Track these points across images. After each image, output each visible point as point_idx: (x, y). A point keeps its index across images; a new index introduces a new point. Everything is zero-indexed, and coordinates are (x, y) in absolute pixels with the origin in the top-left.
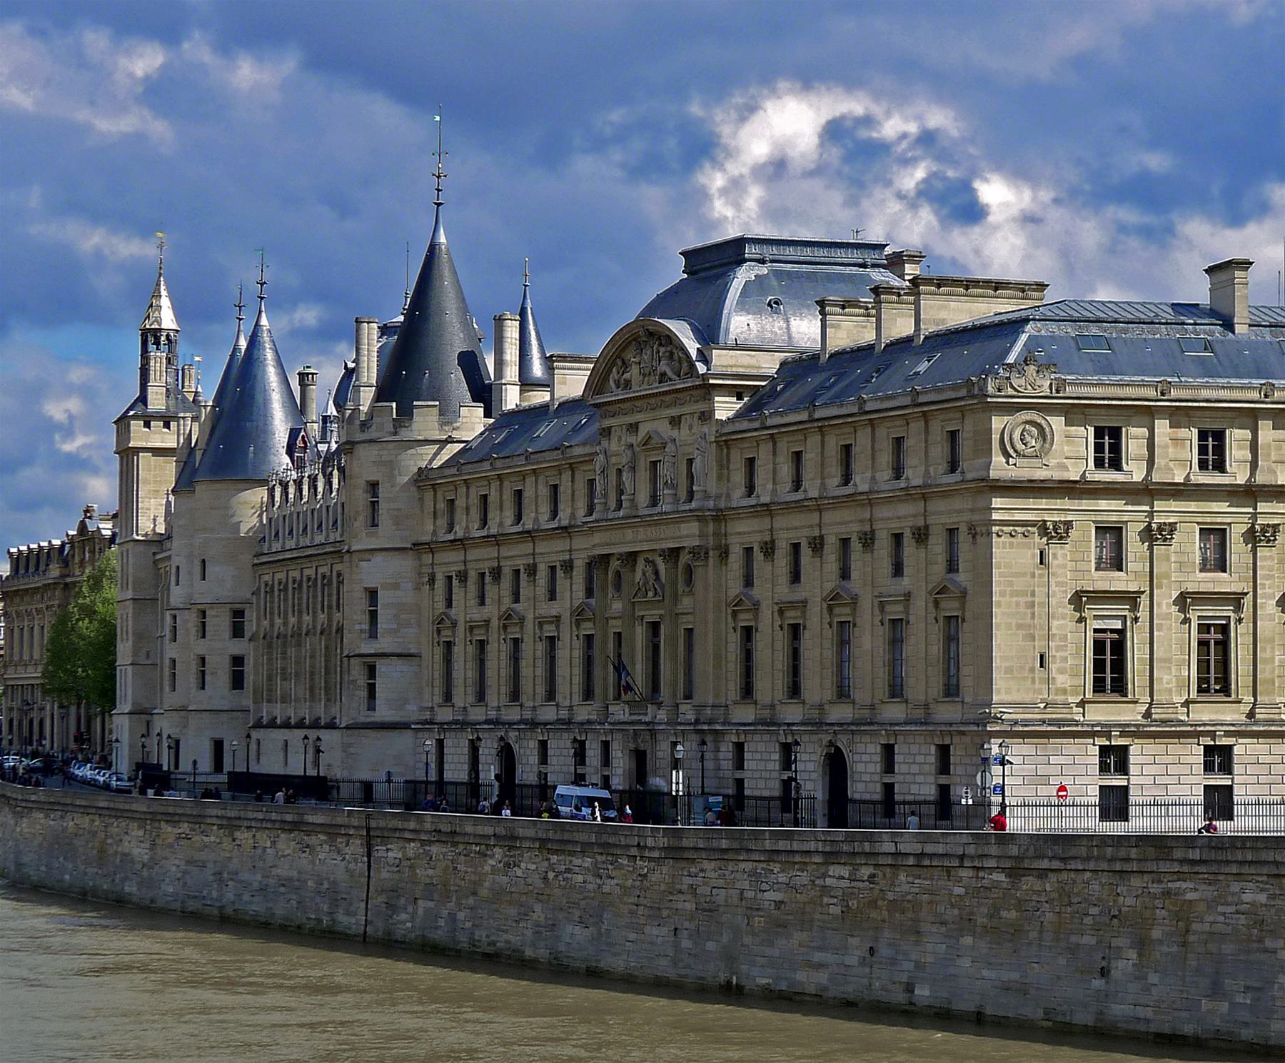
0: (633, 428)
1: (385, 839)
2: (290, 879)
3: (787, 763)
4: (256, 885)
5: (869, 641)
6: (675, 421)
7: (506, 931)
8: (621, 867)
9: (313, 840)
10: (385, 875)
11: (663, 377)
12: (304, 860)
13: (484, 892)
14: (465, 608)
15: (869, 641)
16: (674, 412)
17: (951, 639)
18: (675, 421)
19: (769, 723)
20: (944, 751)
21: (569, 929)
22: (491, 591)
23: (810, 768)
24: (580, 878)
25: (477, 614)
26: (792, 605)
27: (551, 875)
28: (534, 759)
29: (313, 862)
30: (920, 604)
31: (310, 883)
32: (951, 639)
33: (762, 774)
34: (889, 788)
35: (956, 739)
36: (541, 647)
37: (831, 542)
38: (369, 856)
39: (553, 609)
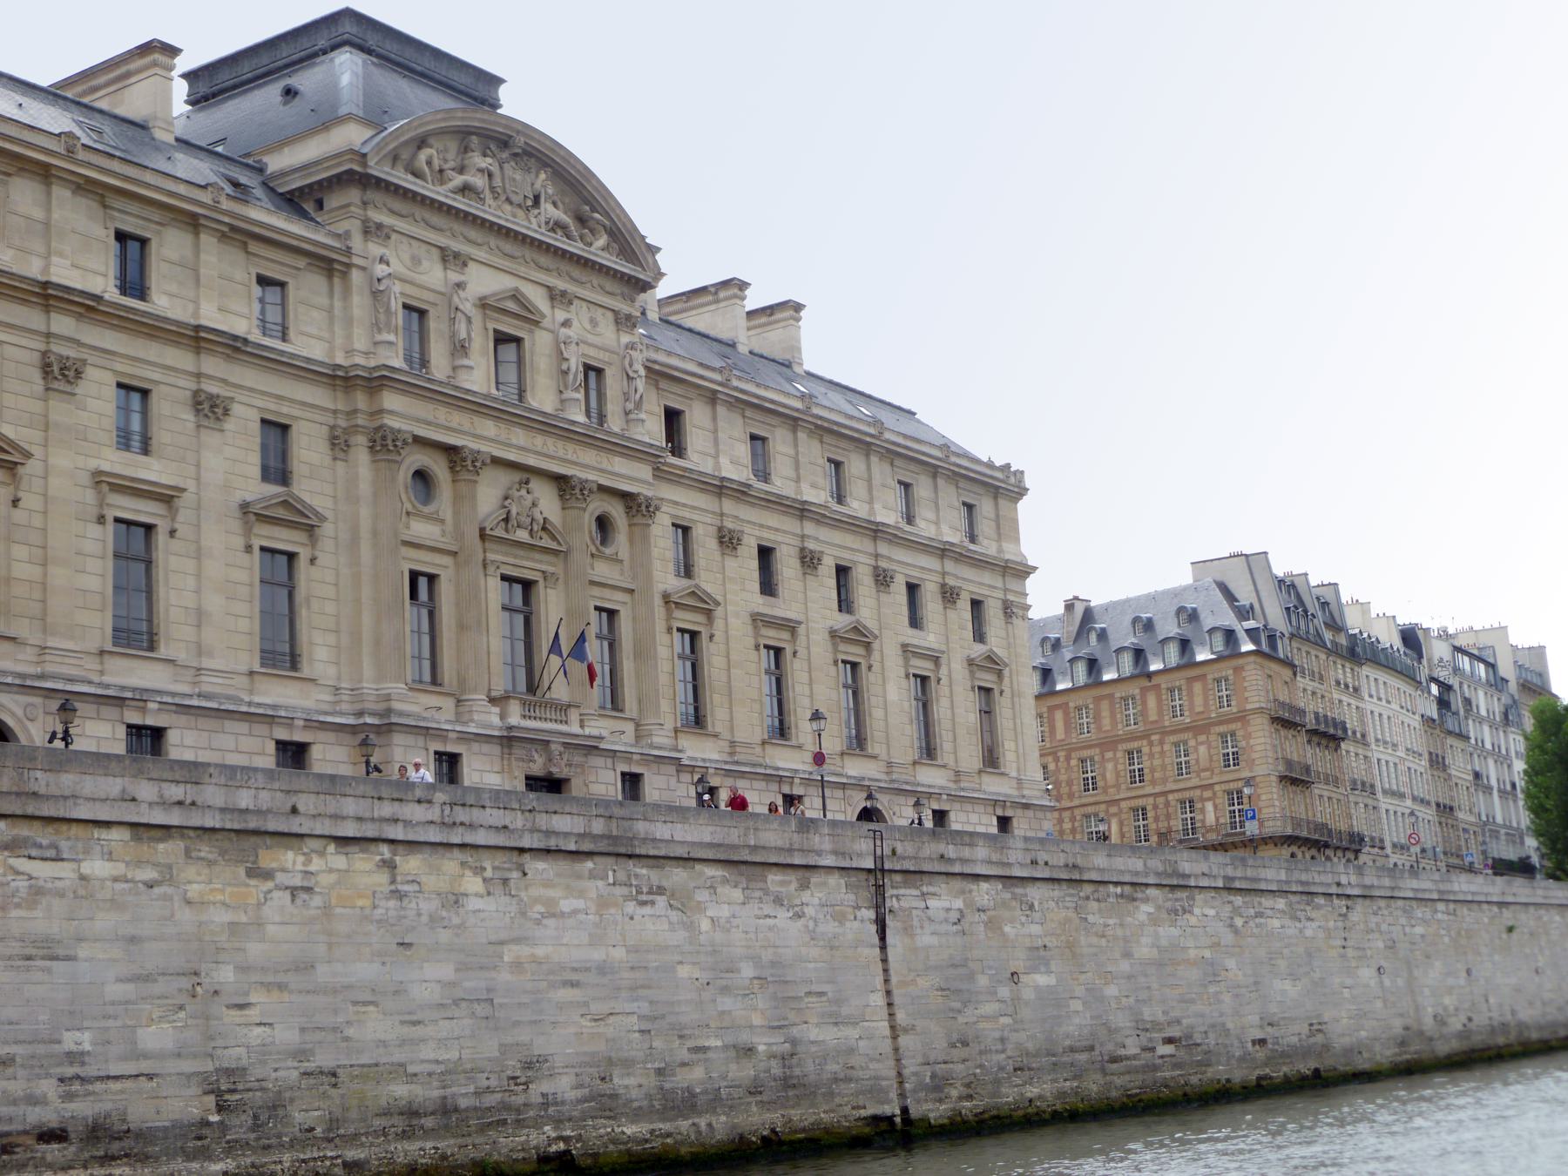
1: (913, 875)
2: (602, 969)
4: (424, 993)
7: (1192, 1001)
8: (1318, 907)
10: (925, 939)
11: (557, 226)
12: (653, 923)
13: (1144, 950)
16: (560, 284)
17: (987, 713)
21: (1278, 984)
24: (1276, 923)
27: (1239, 922)
29: (691, 927)
31: (684, 972)
32: (987, 713)
35: (1019, 812)
36: (99, 541)
38: (879, 904)
39: (152, 470)
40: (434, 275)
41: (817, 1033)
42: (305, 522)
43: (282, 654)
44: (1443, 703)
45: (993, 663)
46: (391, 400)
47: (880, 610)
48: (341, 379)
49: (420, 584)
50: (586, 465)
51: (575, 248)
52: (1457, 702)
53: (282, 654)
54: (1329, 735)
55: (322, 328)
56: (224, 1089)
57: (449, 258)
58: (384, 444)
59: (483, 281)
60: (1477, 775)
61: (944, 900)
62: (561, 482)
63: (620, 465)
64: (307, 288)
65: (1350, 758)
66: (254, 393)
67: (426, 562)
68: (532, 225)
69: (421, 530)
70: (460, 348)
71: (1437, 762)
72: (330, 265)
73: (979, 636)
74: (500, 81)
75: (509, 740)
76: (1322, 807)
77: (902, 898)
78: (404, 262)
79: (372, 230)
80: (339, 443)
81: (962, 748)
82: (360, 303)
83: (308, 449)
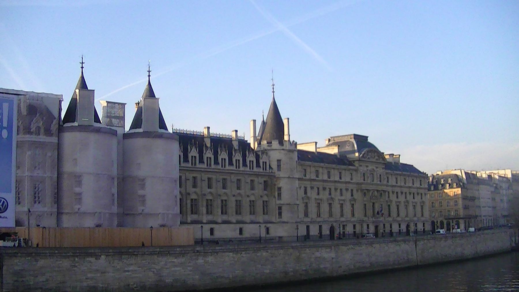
0: (367, 166)
1: (419, 241)
3: (400, 227)
5: (411, 208)
6: (377, 168)
9: (399, 243)
11: (377, 159)
12: (398, 248)
14: (313, 194)
15: (411, 208)
17: (422, 209)
18: (377, 168)
19: (394, 220)
20: (424, 224)
22: (321, 192)
23: (404, 228)
25: (317, 197)
26: (318, 199)
28: (342, 228)
30: (419, 204)
33: (395, 228)
34: (400, 230)
37: (327, 188)
39: (343, 198)
40: (365, 169)
41: (410, 257)
42: (355, 200)
43: (353, 215)
44: (496, 188)
45: (423, 202)
46: (363, 185)
47: (410, 198)
48: (357, 184)
49: (365, 205)
50: (380, 188)
51: (379, 161)
52: (498, 187)
53: (353, 215)
54: (473, 199)
55: (357, 178)
56: (371, 264)
57: (367, 166)
58: (362, 190)
59: (370, 168)
60: (501, 200)
61: (422, 242)
62: (377, 191)
63: (383, 187)
64: (354, 173)
65: (477, 202)
66: (350, 187)
67: (365, 203)
68: (374, 160)
69: (365, 199)
70: (368, 177)
71: (494, 199)
72: (356, 170)
73: (422, 198)
74: (367, 137)
75: (373, 222)
76: (471, 212)
77: (418, 243)
78: (363, 169)
79: (361, 166)
80: (357, 191)
81: (419, 214)
82: (359, 175)
83: (355, 192)
